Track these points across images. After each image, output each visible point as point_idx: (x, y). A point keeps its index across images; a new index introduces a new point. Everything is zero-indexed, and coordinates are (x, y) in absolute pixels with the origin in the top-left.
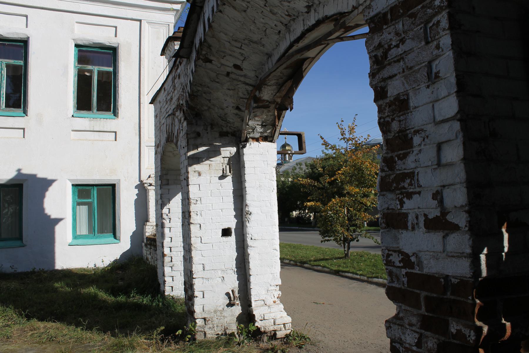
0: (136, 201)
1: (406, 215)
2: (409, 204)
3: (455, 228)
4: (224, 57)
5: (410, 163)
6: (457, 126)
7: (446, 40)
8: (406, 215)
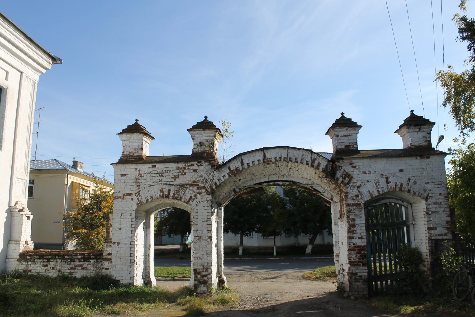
0: (5, 223)
1: (354, 237)
2: (354, 235)
3: (364, 238)
5: (355, 229)
6: (365, 225)
7: (364, 213)
8: (354, 237)
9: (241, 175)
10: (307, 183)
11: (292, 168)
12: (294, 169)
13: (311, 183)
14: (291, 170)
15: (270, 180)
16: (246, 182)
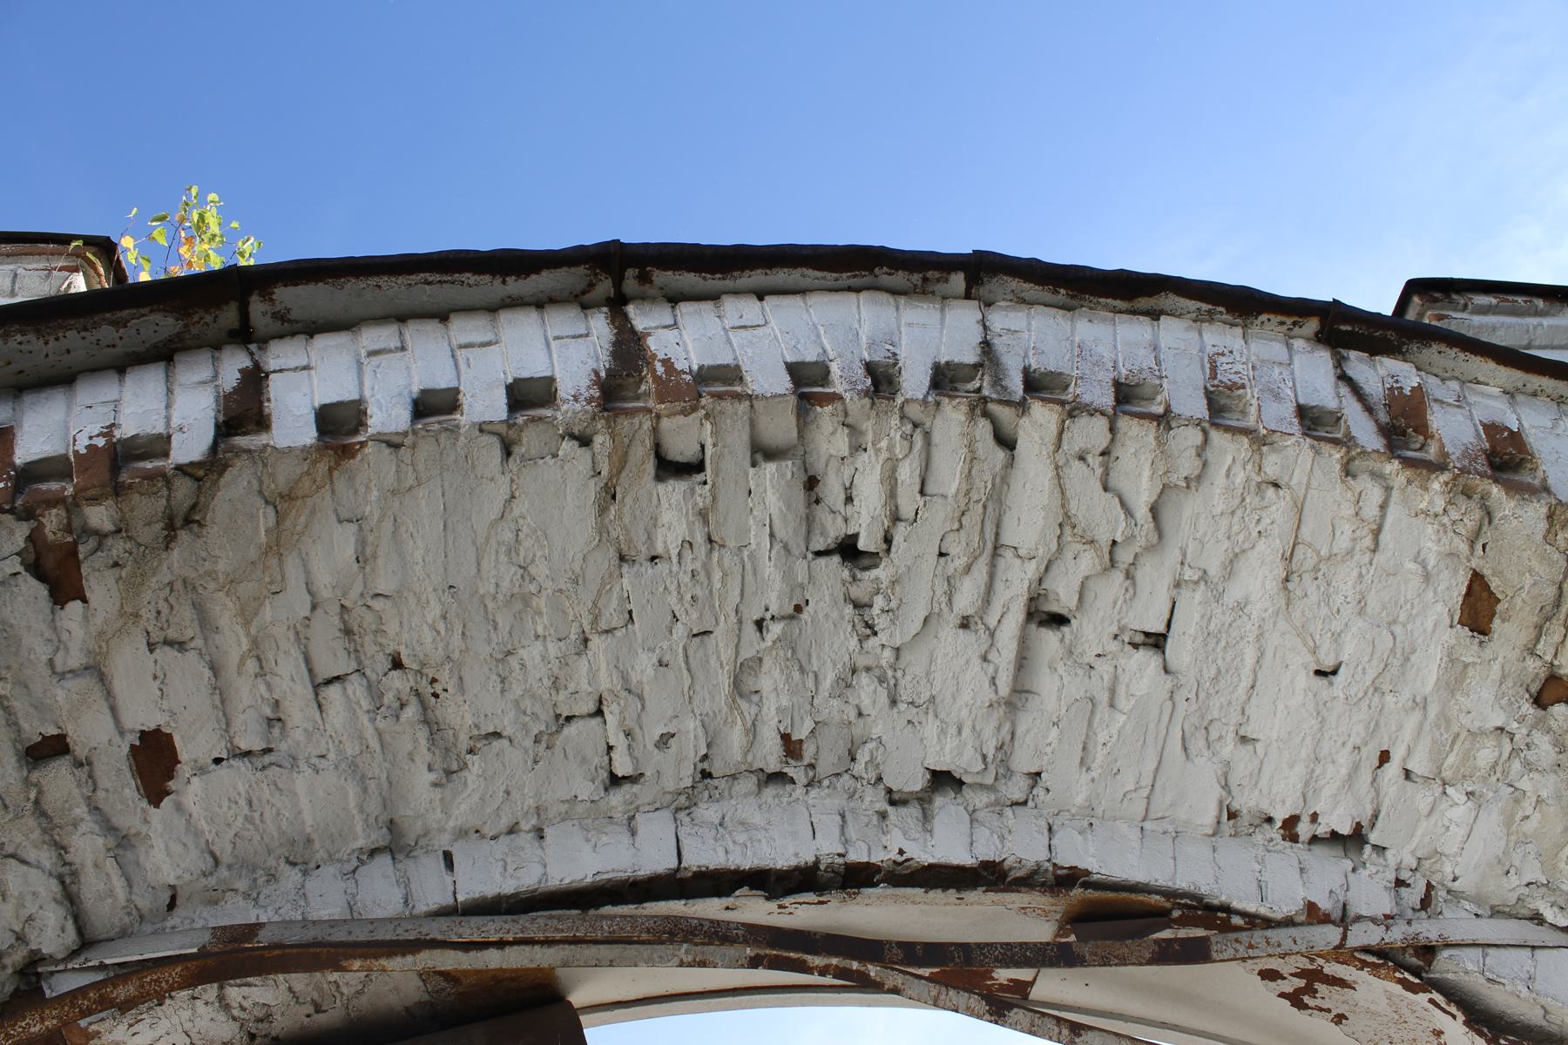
4: (168, 643)
9: (184, 623)
10: (1325, 904)
11: (1063, 596)
12: (1092, 631)
13: (1383, 903)
14: (1049, 639)
15: (704, 855)
16: (292, 877)
